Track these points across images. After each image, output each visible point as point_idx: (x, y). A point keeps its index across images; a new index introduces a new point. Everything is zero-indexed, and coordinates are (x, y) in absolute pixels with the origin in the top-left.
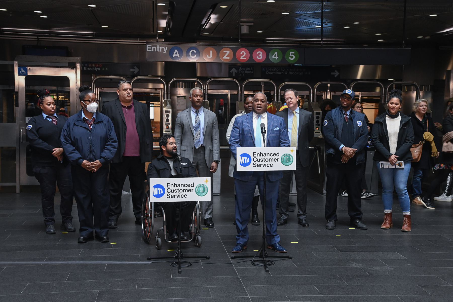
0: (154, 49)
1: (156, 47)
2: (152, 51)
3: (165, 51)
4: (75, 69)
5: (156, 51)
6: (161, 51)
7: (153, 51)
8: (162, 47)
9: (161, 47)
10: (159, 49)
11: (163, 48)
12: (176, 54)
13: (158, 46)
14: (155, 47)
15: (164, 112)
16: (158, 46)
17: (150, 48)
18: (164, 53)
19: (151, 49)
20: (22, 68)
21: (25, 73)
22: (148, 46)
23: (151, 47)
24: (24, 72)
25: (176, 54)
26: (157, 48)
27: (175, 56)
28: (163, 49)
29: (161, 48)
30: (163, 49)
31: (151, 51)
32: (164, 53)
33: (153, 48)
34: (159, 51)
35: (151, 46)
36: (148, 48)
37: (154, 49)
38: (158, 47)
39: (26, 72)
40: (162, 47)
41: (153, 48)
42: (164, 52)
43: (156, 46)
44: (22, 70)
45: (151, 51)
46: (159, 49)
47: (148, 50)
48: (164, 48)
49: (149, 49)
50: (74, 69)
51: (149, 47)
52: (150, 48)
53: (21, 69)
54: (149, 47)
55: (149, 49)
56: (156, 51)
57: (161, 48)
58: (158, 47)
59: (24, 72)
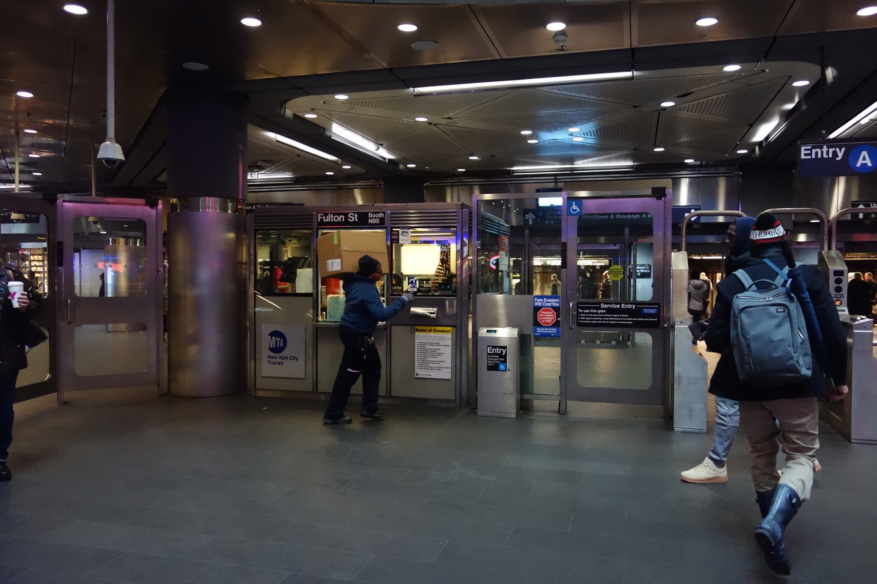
0: (817, 153)
1: (821, 150)
2: (812, 157)
3: (840, 155)
4: (663, 198)
5: (819, 156)
6: (831, 156)
7: (814, 156)
8: (834, 149)
9: (832, 148)
10: (828, 153)
11: (836, 150)
12: (864, 159)
13: (825, 147)
14: (819, 150)
15: (831, 274)
16: (825, 147)
17: (809, 152)
18: (837, 159)
19: (810, 154)
20: (574, 203)
21: (579, 211)
22: (803, 148)
23: (811, 150)
24: (577, 208)
25: (864, 159)
26: (822, 152)
27: (862, 164)
28: (835, 153)
29: (831, 150)
30: (835, 153)
31: (809, 157)
32: (837, 159)
33: (814, 151)
34: (827, 157)
35: (810, 147)
36: (803, 152)
37: (817, 153)
38: (825, 149)
39: (580, 210)
40: (834, 149)
41: (814, 151)
42: (838, 157)
43: (821, 148)
44: (574, 205)
45: (809, 157)
46: (828, 153)
47: (803, 157)
48: (838, 150)
49: (806, 155)
50: (661, 199)
51: (805, 150)
52: (809, 152)
53: (573, 204)
54: (805, 150)
55: (806, 155)
56: (819, 156)
57: (831, 150)
58: (825, 149)
59: (577, 210)
